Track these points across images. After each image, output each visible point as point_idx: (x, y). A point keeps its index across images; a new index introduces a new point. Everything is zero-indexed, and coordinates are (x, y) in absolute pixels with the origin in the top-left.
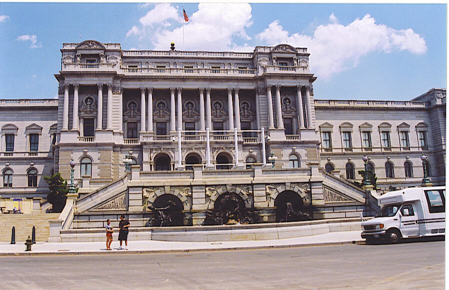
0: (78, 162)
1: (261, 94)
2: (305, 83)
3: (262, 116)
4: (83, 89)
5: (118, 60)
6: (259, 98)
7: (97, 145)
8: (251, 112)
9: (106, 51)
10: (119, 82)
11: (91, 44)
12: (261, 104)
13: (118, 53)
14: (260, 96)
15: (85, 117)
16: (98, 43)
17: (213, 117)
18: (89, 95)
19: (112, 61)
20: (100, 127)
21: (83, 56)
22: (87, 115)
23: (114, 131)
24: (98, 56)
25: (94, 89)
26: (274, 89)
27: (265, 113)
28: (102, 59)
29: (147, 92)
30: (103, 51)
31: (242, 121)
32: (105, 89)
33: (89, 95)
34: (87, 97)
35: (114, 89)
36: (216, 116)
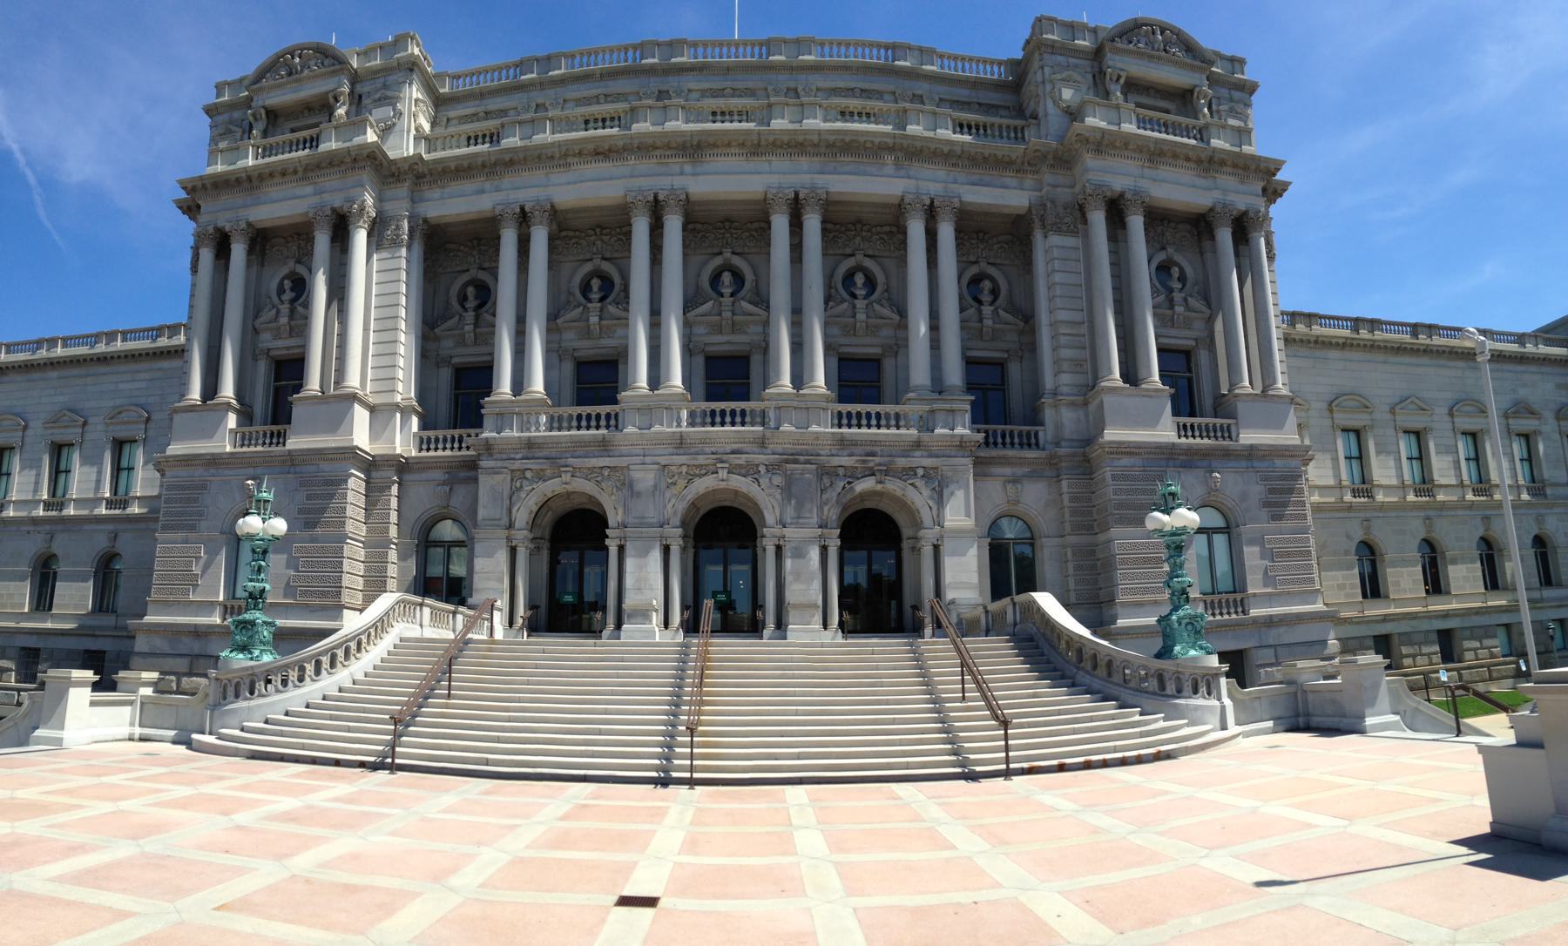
1: (1059, 231)
2: (1243, 197)
3: (1062, 330)
6: (1048, 249)
8: (1009, 317)
10: (403, 190)
12: (1058, 278)
14: (1055, 239)
17: (835, 331)
18: (291, 264)
26: (1116, 210)
27: (1077, 317)
29: (524, 219)
31: (970, 353)
33: (291, 264)
34: (285, 271)
36: (850, 330)
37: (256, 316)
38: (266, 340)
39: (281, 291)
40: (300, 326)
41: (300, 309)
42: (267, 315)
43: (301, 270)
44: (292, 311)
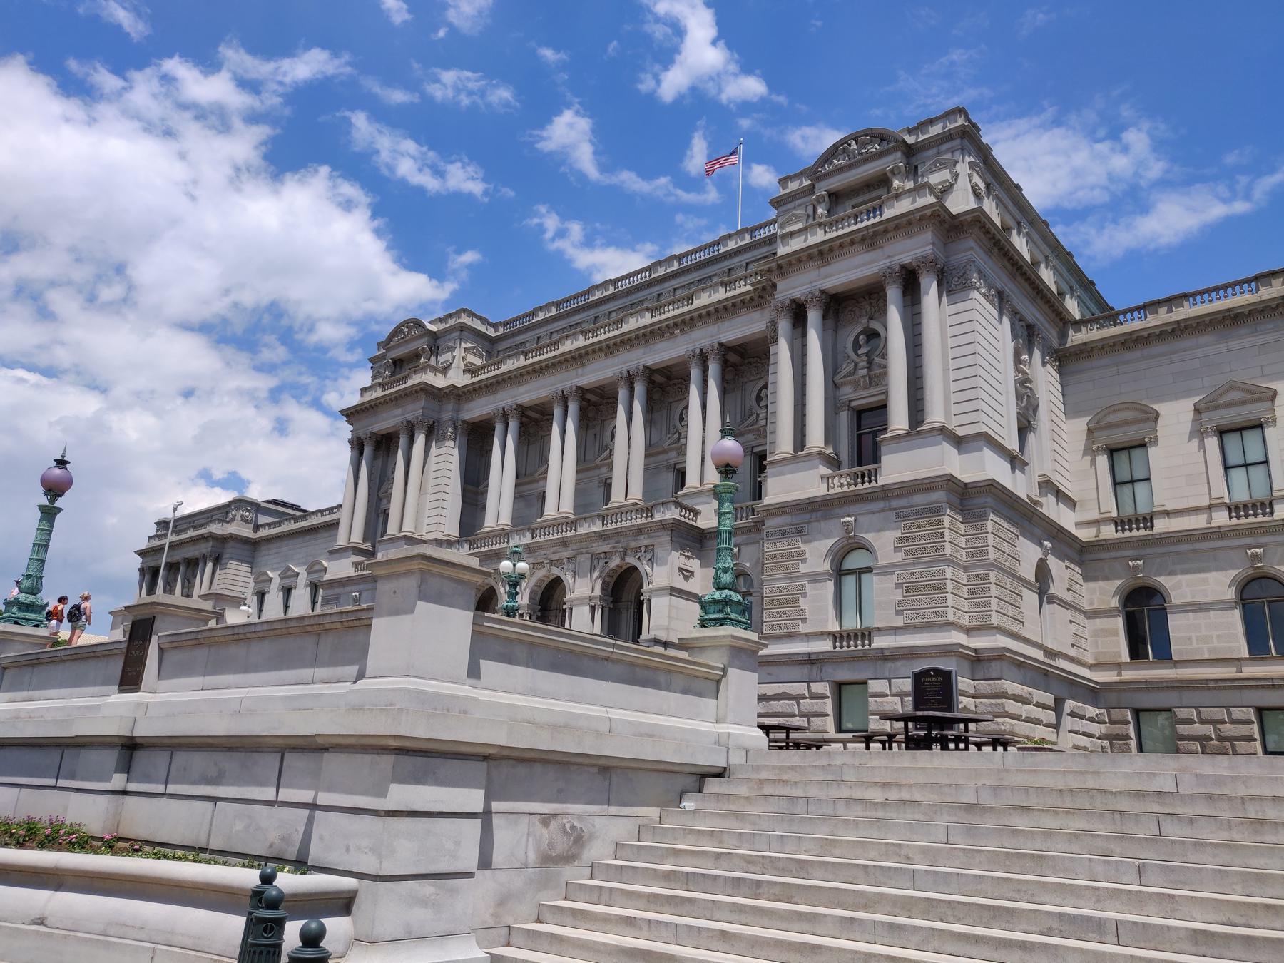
0: (826, 566)
4: (837, 305)
5: (959, 168)
7: (887, 493)
9: (910, 152)
11: (854, 146)
13: (958, 142)
15: (853, 404)
16: (882, 137)
18: (864, 320)
19: (935, 179)
20: (899, 419)
21: (835, 198)
22: (863, 394)
23: (961, 432)
24: (882, 181)
25: (866, 298)
28: (896, 183)
30: (899, 154)
32: (910, 281)
33: (864, 320)
34: (860, 329)
35: (952, 284)
37: (835, 372)
38: (847, 392)
39: (856, 346)
40: (878, 376)
41: (878, 360)
42: (846, 368)
43: (874, 325)
44: (870, 363)
